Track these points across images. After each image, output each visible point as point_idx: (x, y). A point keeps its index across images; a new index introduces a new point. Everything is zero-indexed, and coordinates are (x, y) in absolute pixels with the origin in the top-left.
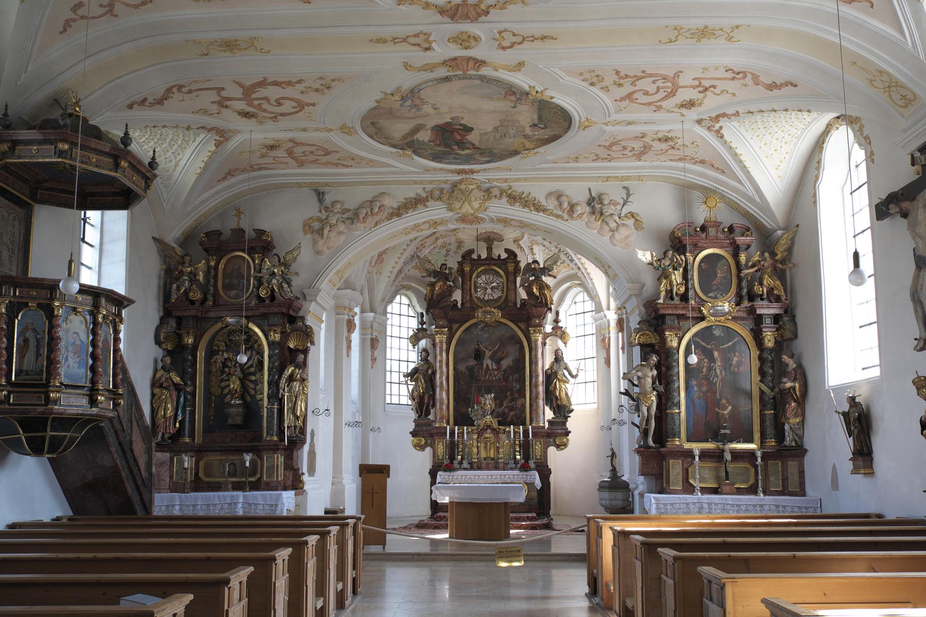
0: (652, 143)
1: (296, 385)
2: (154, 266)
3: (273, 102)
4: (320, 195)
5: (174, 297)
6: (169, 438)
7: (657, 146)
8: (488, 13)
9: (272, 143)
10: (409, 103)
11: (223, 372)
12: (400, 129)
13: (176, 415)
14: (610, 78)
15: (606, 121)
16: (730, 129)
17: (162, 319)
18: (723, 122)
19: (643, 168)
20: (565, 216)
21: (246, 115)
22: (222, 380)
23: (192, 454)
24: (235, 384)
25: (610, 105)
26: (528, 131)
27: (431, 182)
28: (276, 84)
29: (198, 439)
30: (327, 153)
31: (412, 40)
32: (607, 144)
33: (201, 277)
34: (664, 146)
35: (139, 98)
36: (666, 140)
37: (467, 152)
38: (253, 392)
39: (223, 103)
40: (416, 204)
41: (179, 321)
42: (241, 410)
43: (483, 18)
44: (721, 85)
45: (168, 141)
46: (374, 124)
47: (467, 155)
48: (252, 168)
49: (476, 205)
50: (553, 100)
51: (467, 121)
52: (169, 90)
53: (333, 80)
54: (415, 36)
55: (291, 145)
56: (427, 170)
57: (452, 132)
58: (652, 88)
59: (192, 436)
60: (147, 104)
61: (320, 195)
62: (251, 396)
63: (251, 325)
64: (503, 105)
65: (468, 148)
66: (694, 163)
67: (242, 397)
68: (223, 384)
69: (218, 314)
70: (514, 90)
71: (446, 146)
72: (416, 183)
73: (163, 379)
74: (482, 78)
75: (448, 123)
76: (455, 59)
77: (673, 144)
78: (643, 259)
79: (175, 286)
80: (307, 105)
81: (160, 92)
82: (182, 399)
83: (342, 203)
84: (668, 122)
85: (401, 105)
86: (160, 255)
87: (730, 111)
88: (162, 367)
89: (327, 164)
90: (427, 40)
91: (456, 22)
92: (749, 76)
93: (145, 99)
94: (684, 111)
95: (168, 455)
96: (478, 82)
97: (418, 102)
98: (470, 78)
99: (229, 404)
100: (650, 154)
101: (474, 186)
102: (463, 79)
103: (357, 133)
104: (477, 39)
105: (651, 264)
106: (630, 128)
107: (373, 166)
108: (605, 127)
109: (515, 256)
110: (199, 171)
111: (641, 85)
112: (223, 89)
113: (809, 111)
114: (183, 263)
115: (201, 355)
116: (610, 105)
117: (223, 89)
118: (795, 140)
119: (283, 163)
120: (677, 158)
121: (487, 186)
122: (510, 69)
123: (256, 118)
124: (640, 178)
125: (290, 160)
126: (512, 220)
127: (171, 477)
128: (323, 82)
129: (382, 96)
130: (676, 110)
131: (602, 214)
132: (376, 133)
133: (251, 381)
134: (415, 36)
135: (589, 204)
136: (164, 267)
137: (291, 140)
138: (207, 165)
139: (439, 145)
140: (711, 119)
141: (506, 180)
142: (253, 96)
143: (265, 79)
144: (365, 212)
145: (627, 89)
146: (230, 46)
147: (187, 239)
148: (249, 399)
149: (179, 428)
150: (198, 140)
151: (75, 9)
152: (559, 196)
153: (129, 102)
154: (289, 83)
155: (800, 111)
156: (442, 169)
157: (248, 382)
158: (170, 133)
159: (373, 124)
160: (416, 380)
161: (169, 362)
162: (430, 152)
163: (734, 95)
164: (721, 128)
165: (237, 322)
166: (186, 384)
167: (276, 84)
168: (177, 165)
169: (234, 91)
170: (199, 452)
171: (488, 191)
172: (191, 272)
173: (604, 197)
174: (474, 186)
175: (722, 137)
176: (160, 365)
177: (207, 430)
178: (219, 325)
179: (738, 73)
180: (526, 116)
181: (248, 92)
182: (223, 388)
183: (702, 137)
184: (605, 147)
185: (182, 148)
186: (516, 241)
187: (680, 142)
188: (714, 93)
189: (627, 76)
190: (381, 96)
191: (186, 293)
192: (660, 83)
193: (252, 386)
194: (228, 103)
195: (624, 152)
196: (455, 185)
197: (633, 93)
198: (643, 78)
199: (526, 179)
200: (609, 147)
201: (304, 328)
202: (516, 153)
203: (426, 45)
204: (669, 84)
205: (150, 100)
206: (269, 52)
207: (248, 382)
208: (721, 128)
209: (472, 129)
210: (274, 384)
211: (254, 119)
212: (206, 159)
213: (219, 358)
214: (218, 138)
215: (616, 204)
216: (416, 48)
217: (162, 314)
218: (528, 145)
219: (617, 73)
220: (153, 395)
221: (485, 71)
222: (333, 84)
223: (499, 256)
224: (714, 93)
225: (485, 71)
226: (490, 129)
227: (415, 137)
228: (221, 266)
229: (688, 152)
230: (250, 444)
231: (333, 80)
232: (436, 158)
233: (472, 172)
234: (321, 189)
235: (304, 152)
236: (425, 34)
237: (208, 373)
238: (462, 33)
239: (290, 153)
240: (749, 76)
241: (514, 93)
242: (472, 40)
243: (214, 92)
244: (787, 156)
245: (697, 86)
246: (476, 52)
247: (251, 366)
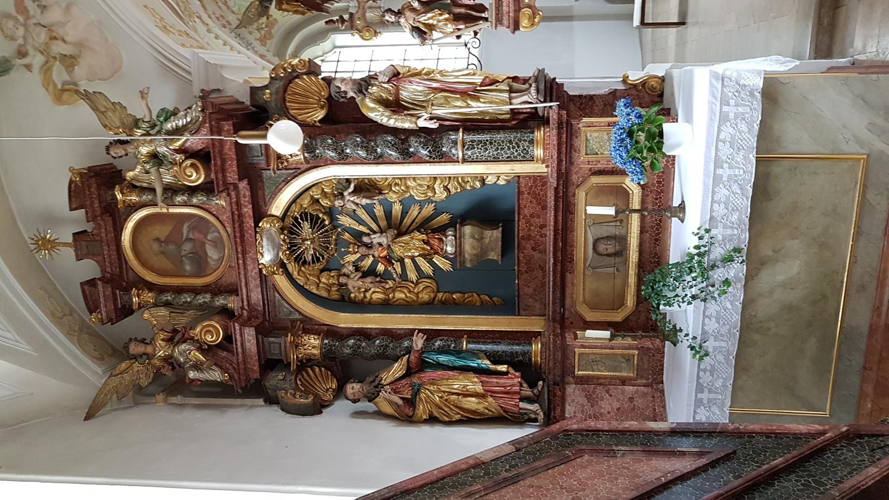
1: (410, 91)
2: (162, 420)
5: (216, 375)
6: (532, 385)
11: (385, 277)
13: (480, 371)
17: (271, 401)
22: (404, 276)
23: (569, 337)
24: (411, 246)
29: (535, 324)
33: (182, 320)
38: (428, 210)
41: (270, 364)
42: (467, 229)
59: (528, 337)
62: (437, 213)
63: (278, 207)
67: (442, 230)
68: (412, 275)
69: (255, 283)
73: (396, 399)
79: (192, 374)
82: (443, 359)
86: (136, 404)
88: (370, 400)
95: (570, 389)
99: (457, 259)
114: (150, 357)
115: (346, 320)
127: (624, 382)
133: (404, 213)
136: (160, 397)
147: (114, 353)
148: (444, 218)
149: (510, 364)
157: (407, 221)
160: (432, 27)
161: (357, 386)
165: (272, 240)
166: (409, 350)
170: (565, 322)
172: (170, 340)
176: (364, 405)
177: (509, 307)
178: (281, 281)
182: (421, 274)
191: (207, 350)
193: (414, 211)
201: (279, 84)
207: (407, 221)
210: (403, 144)
213: (355, 285)
217: (261, 401)
220: (432, 420)
228: (150, 277)
230: (551, 202)
237: (386, 306)
247: (369, 210)
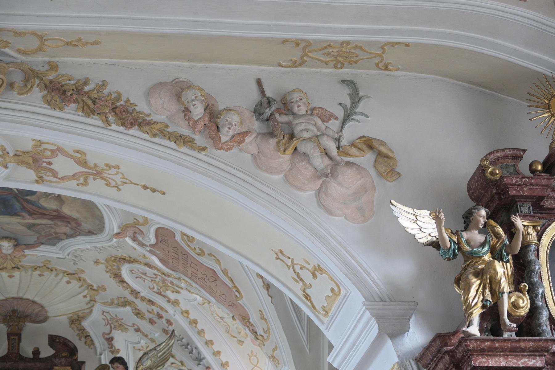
20: (199, 140)
78: (412, 228)
105: (436, 245)
109: (73, 351)
126: (58, 151)
131: (292, 136)
135: (258, 112)
173: (296, 96)
186: (76, 320)
215: (326, 117)
223: (36, 352)
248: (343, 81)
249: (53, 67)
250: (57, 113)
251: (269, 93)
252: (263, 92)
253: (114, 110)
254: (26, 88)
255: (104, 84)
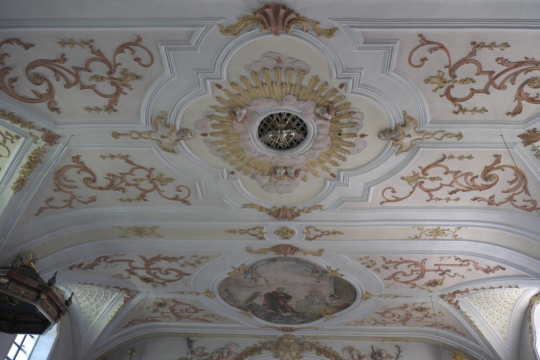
0: (412, 312)
3: (163, 272)
4: (190, 342)
7: (416, 314)
8: (299, 215)
9: (161, 301)
10: (249, 276)
12: (243, 295)
14: (380, 263)
15: (379, 294)
16: (464, 302)
18: (458, 297)
19: (408, 331)
21: (146, 280)
25: (381, 282)
26: (328, 300)
27: (265, 337)
28: (166, 259)
30: (197, 311)
31: (252, 232)
32: (382, 311)
34: (420, 315)
35: (77, 263)
36: (421, 310)
37: (288, 314)
39: (132, 271)
40: (253, 352)
43: (296, 218)
44: (454, 270)
45: (95, 296)
46: (227, 290)
47: (289, 317)
48: (147, 320)
49: (294, 354)
50: (343, 277)
51: (287, 291)
52: (98, 259)
53: (202, 258)
54: (253, 229)
55: (173, 304)
56: (262, 327)
57: (278, 299)
58: (408, 271)
60: (82, 267)
61: (190, 342)
64: (310, 280)
65: (289, 312)
66: (443, 328)
70: (317, 269)
71: (274, 309)
72: (254, 336)
74: (297, 260)
75: (275, 292)
76: (278, 246)
77: (426, 313)
80: (185, 274)
81: (92, 260)
83: (203, 348)
84: (421, 297)
85: (245, 278)
87: (462, 289)
89: (196, 319)
90: (261, 232)
91: (279, 220)
92: (472, 263)
93: (82, 264)
94: (431, 288)
96: (294, 263)
97: (255, 276)
98: (289, 260)
100: (411, 321)
101: (293, 341)
102: (284, 260)
103: (215, 297)
104: (292, 232)
106: (396, 300)
107: (226, 322)
108: (379, 299)
110: (110, 319)
111: (401, 267)
112: (132, 261)
113: (517, 287)
116: (381, 282)
117: (132, 261)
118: (510, 312)
119: (167, 317)
120: (430, 324)
121: (302, 341)
122: (314, 254)
123: (152, 282)
124: (406, 340)
125: (172, 315)
128: (196, 259)
129: (233, 270)
130: (426, 287)
132: (228, 298)
134: (253, 229)
137: (174, 300)
138: (117, 314)
139: (269, 308)
140: (450, 295)
141: (315, 337)
142: (152, 266)
143: (160, 255)
144: (218, 356)
145: (392, 271)
146: (140, 232)
150: (114, 297)
151: (47, 201)
152: (350, 350)
153: (71, 265)
154: (175, 259)
155: (510, 287)
156: (271, 327)
158: (96, 289)
159: (226, 290)
162: (263, 313)
163: (463, 277)
164: (457, 301)
167: (166, 259)
168: (97, 314)
169: (139, 263)
171: (302, 344)
173: (382, 352)
174: (293, 341)
175: (459, 308)
179: (464, 261)
180: (326, 288)
181: (148, 263)
183: (446, 309)
184: (380, 314)
185: (103, 302)
187: (431, 312)
188: (449, 275)
189: (391, 262)
190: (231, 270)
192: (413, 267)
194: (135, 271)
195: (394, 318)
196: (281, 339)
197: (395, 274)
198: (401, 263)
199: (328, 337)
200: (383, 314)
202: (320, 316)
203: (260, 236)
204: (419, 268)
205: (85, 265)
206: (163, 237)
208: (457, 301)
209: (291, 297)
211: (150, 284)
212: (116, 310)
214: (126, 296)
216: (254, 237)
218: (328, 310)
219: (384, 259)
221: (298, 255)
222: (202, 260)
224: (449, 275)
225: (298, 255)
226: (303, 298)
227: (254, 302)
229: (438, 319)
231: (202, 258)
232: (267, 318)
233: (292, 330)
234: (191, 339)
235: (181, 310)
236: (260, 228)
238: (283, 228)
239: (172, 310)
240: (472, 263)
241: (318, 272)
242: (290, 233)
243: (127, 263)
244: (507, 324)
245: (438, 270)
246: (292, 242)
248: (396, 346)
249: (318, 343)
250: (319, 357)
251: (375, 350)
252: (373, 350)
253: (334, 356)
254: (311, 350)
255: (331, 348)
